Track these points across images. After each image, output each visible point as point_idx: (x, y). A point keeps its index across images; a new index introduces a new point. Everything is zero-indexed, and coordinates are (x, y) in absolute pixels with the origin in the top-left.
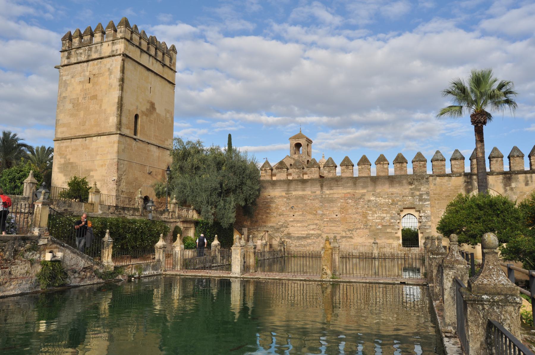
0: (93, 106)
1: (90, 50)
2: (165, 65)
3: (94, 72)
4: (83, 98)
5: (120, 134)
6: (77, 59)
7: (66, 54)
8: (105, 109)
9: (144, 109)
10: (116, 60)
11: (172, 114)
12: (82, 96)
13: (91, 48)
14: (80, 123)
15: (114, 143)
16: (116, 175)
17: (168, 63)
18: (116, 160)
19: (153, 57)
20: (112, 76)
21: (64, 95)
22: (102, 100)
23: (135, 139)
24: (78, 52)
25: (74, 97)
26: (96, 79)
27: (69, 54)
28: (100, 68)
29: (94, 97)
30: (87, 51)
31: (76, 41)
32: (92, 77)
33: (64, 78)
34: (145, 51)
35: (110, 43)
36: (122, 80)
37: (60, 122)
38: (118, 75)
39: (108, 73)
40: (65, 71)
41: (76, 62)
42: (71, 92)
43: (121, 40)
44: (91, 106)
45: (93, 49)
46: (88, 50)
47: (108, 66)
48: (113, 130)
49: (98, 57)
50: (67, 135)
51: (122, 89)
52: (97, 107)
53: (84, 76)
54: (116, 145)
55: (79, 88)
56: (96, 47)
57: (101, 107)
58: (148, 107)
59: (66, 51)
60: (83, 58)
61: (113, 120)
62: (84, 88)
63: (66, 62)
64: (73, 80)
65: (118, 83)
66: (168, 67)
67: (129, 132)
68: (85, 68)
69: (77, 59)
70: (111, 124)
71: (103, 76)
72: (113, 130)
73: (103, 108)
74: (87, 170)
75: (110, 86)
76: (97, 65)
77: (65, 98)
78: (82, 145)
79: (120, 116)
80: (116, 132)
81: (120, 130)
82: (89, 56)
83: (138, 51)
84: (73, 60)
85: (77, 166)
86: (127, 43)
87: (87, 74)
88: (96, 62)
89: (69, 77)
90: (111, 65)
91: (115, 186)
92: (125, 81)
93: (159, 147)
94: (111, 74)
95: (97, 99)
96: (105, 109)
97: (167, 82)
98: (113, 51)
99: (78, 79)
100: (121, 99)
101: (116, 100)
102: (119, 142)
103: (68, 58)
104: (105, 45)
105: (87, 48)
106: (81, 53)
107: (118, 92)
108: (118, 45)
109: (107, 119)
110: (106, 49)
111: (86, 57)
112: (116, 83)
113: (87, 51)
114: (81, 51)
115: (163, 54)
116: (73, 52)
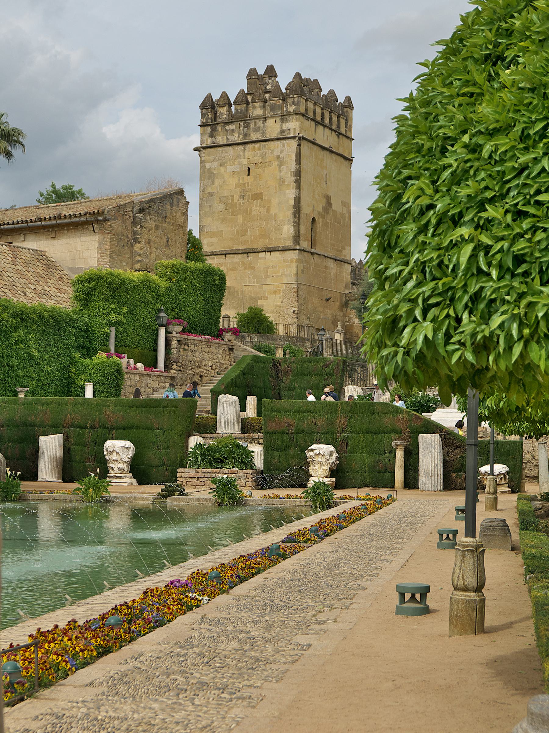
0: (256, 209)
1: (247, 126)
2: (340, 134)
3: (255, 160)
4: (240, 197)
5: (299, 250)
6: (227, 139)
7: (209, 129)
8: (275, 215)
9: (320, 209)
10: (288, 144)
11: (349, 208)
12: (239, 194)
13: (249, 124)
14: (238, 232)
15: (291, 261)
16: (296, 305)
17: (343, 130)
18: (295, 286)
19: (328, 127)
20: (284, 167)
21: (209, 190)
22: (269, 201)
23: (312, 254)
24: (227, 128)
25: (226, 195)
26: (258, 171)
27: (214, 130)
28: (264, 155)
29: (258, 196)
30: (241, 128)
31: (223, 112)
32: (252, 166)
33: (208, 165)
34: (319, 123)
35: (278, 119)
36: (298, 174)
37: (207, 229)
38: (293, 166)
39: (276, 163)
40: (209, 155)
41: (225, 142)
42: (221, 186)
43: (294, 117)
44: (253, 208)
45: (252, 125)
46: (244, 127)
47: (277, 152)
48: (289, 243)
49: (260, 138)
50: (219, 249)
51: (298, 187)
52: (263, 211)
53: (240, 164)
54: (294, 265)
55: (232, 181)
56: (256, 124)
57: (268, 210)
58: (324, 205)
59: (209, 125)
60: (236, 138)
61: (288, 230)
62: (241, 181)
63: (209, 142)
64: (222, 169)
65: (293, 179)
66: (343, 135)
67: (305, 244)
68: (241, 153)
69: (227, 139)
70: (285, 236)
71: (269, 166)
72: (289, 243)
73: (273, 211)
74: (252, 298)
75: (281, 181)
76: (259, 149)
77: (211, 194)
78: (243, 262)
79: (297, 225)
80: (294, 247)
81: (299, 245)
82: (245, 135)
83: (313, 124)
84: (221, 139)
85: (237, 292)
86: (302, 118)
87: (245, 161)
88: (257, 145)
89: (216, 164)
90: (282, 152)
91: (296, 320)
92: (303, 174)
93: (336, 260)
94: (281, 165)
95: (262, 199)
96: (275, 215)
97: (342, 160)
98: (283, 131)
99: (230, 168)
100: (298, 200)
101: (292, 202)
102: (298, 261)
103: (212, 136)
104: (270, 122)
105: (241, 124)
106: (233, 131)
107: (294, 191)
108: (291, 123)
109: (278, 229)
110: (273, 127)
111: (241, 137)
112: (290, 179)
113: (241, 128)
114: (232, 127)
115: (338, 117)
116: (219, 128)
